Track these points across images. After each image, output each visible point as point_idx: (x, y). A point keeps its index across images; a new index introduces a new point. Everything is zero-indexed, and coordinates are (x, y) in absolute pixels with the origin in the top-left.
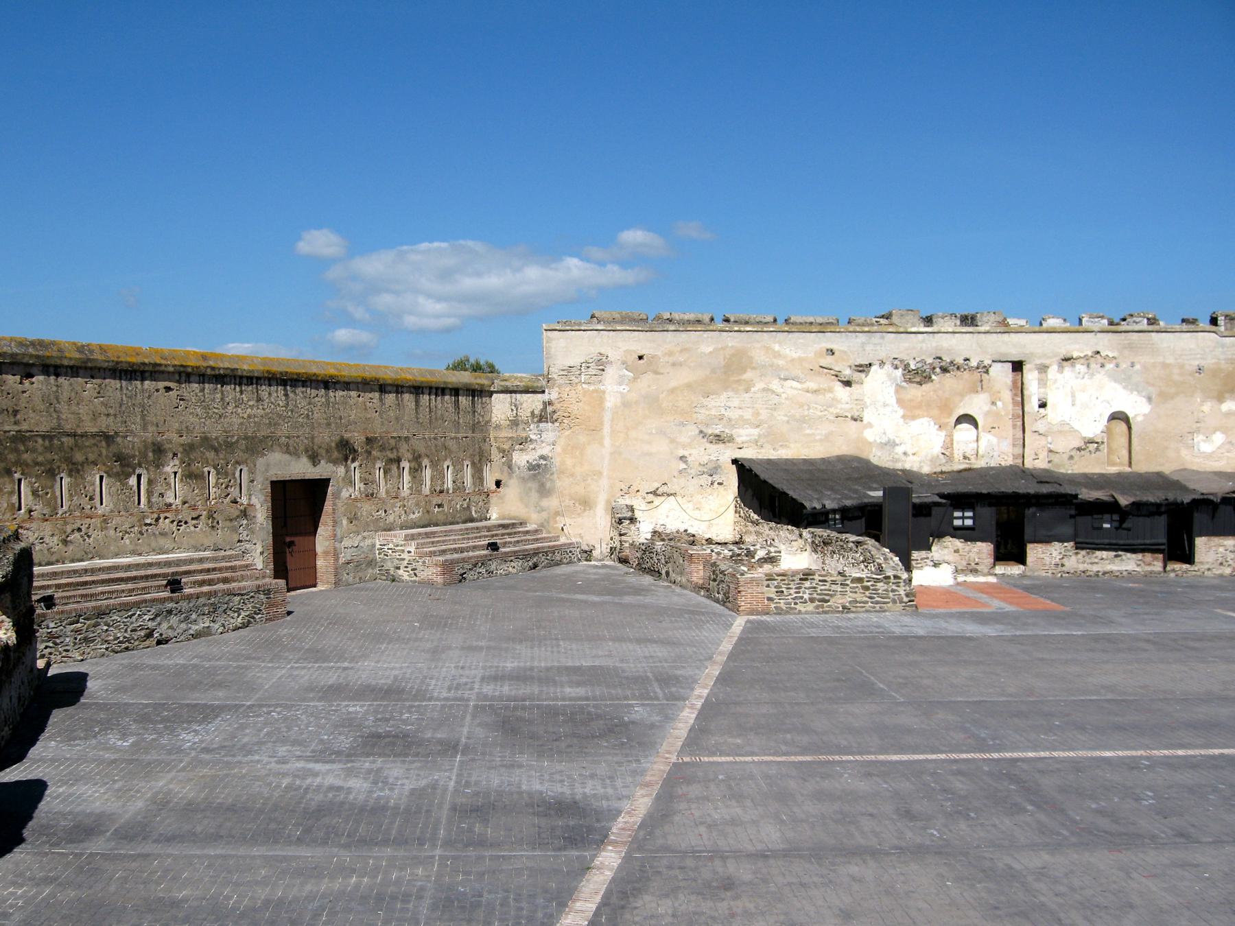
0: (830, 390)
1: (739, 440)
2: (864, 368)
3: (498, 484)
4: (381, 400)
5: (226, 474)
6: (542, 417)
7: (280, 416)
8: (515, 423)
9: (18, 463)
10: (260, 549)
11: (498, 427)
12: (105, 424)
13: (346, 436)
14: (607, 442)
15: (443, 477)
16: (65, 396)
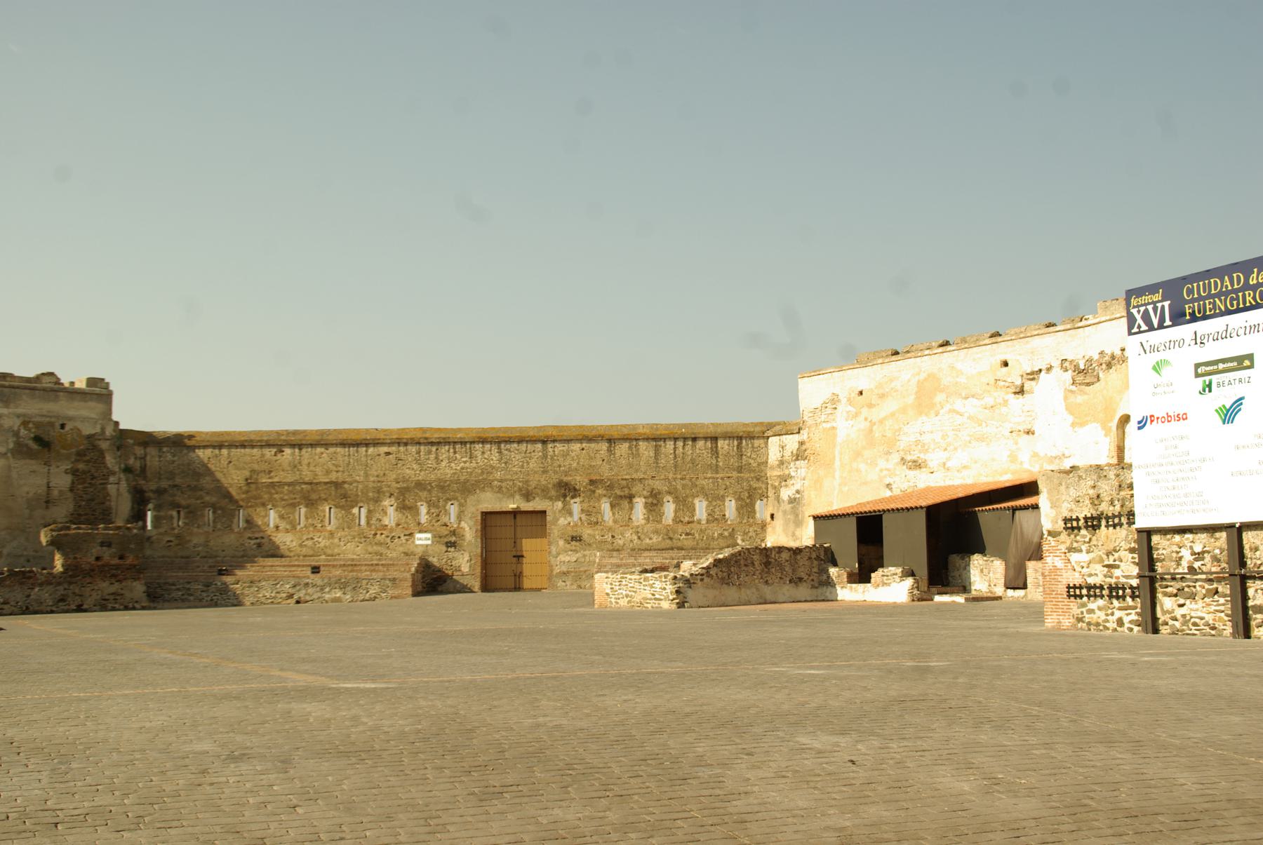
0: (1006, 401)
1: (930, 464)
2: (1034, 375)
3: (772, 516)
4: (609, 450)
5: (438, 507)
6: (799, 456)
7: (493, 467)
8: (782, 463)
9: (271, 500)
10: (467, 558)
11: (772, 468)
12: (339, 477)
13: (565, 479)
14: (837, 474)
15: (692, 510)
16: (305, 462)
